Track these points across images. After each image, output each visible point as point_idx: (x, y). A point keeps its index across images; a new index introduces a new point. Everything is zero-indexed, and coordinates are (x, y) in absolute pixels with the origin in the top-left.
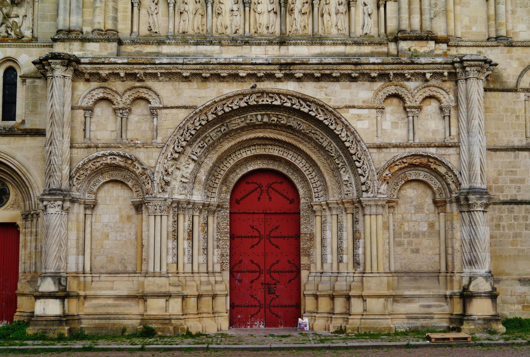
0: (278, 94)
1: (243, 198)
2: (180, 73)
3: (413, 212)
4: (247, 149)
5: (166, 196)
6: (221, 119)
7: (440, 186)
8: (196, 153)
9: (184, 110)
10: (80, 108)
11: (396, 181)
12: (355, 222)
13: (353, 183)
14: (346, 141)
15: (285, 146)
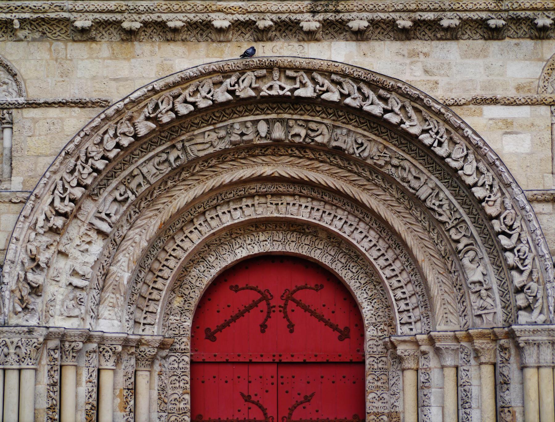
0: (309, 71)
1: (223, 326)
2: (68, 20)
4: (232, 206)
5: (33, 322)
6: (169, 132)
8: (108, 215)
9: (77, 109)
12: (500, 384)
13: (495, 287)
14: (475, 185)
15: (326, 198)
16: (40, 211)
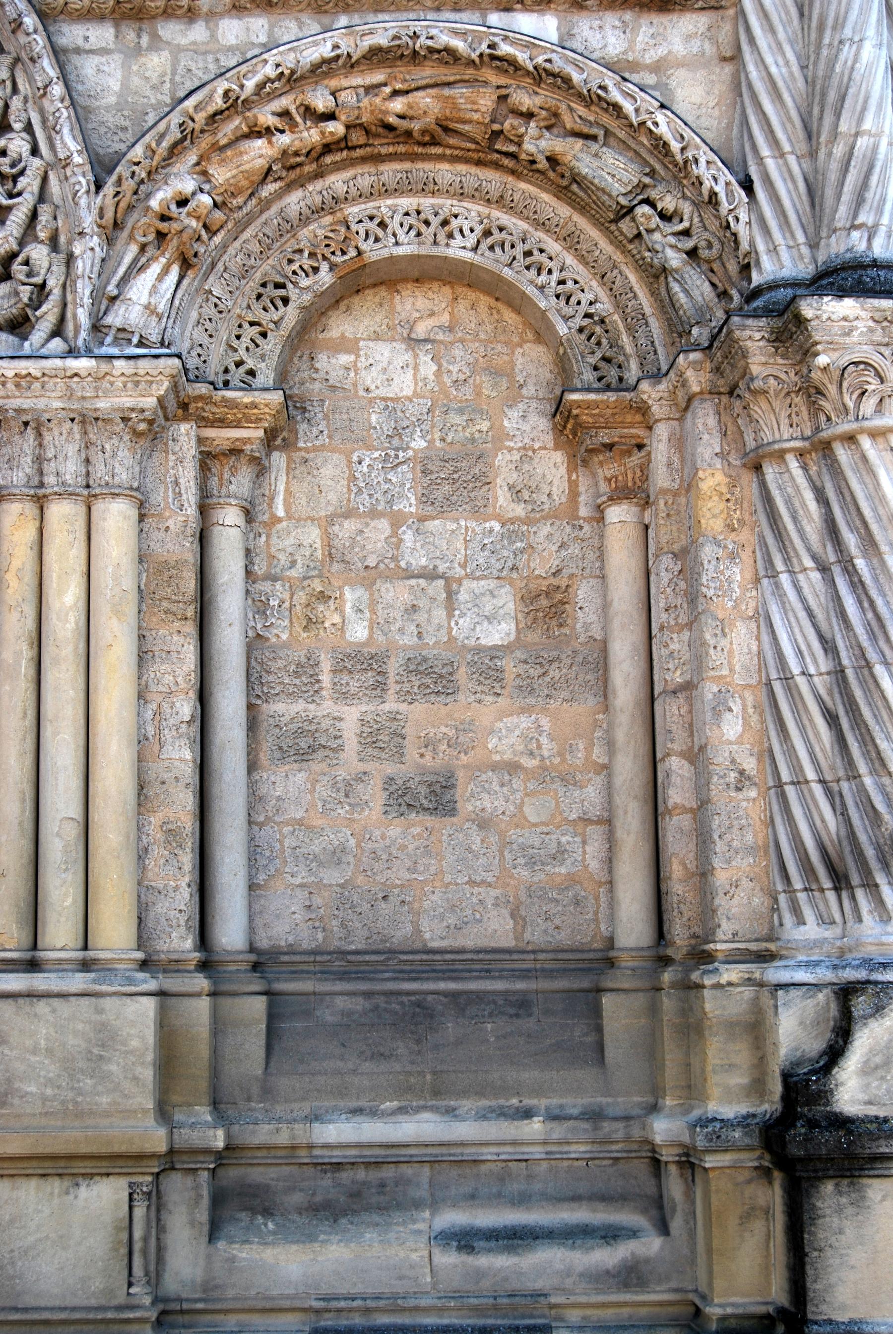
3: (409, 504)
7: (605, 306)
11: (266, 268)
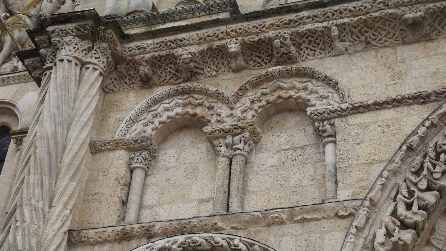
9: (416, 107)
10: (117, 145)
16: (378, 225)
